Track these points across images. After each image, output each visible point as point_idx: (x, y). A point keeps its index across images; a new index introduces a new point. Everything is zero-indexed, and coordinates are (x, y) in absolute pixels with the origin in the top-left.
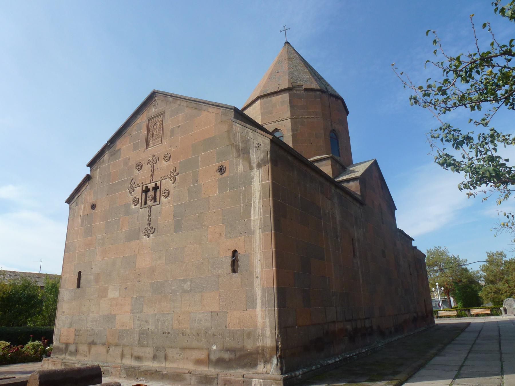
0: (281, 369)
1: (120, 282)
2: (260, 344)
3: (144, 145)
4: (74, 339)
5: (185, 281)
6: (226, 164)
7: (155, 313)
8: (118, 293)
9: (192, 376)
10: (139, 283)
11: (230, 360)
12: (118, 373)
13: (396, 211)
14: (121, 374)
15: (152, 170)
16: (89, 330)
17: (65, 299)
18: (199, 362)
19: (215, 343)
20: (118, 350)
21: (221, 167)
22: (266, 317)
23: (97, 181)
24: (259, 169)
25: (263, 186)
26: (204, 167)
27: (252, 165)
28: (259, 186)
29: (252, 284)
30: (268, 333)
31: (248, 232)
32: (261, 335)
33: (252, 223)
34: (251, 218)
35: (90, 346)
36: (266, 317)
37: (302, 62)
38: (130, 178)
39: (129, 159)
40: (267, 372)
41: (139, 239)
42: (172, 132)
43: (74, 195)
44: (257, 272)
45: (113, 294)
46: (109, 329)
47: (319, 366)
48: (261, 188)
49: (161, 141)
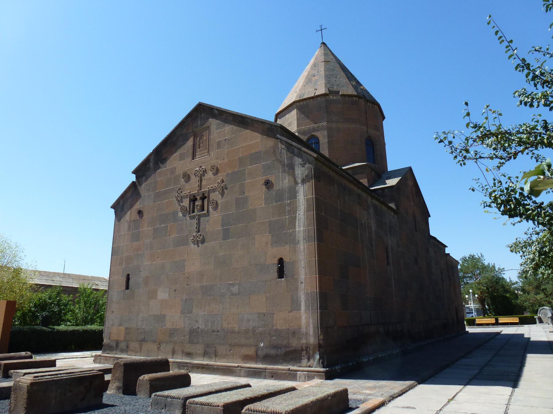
0: (323, 363)
2: (304, 341)
3: (191, 156)
4: (125, 337)
6: (272, 179)
7: (205, 313)
8: (168, 295)
10: (189, 286)
11: (277, 356)
13: (429, 218)
15: (199, 180)
16: (139, 329)
18: (247, 358)
19: (262, 341)
20: (170, 347)
21: (267, 181)
22: (310, 318)
23: (143, 189)
24: (303, 185)
25: (308, 200)
26: (250, 179)
27: (297, 180)
28: (304, 200)
29: (297, 289)
30: (311, 332)
31: (293, 241)
32: (305, 334)
33: (297, 234)
34: (296, 229)
35: (141, 343)
36: (310, 318)
37: (338, 65)
38: (177, 187)
39: (176, 168)
40: (310, 365)
41: (187, 245)
42: (219, 144)
43: (120, 201)
44: (301, 278)
45: (162, 295)
47: (355, 363)
48: (305, 202)
49: (207, 152)
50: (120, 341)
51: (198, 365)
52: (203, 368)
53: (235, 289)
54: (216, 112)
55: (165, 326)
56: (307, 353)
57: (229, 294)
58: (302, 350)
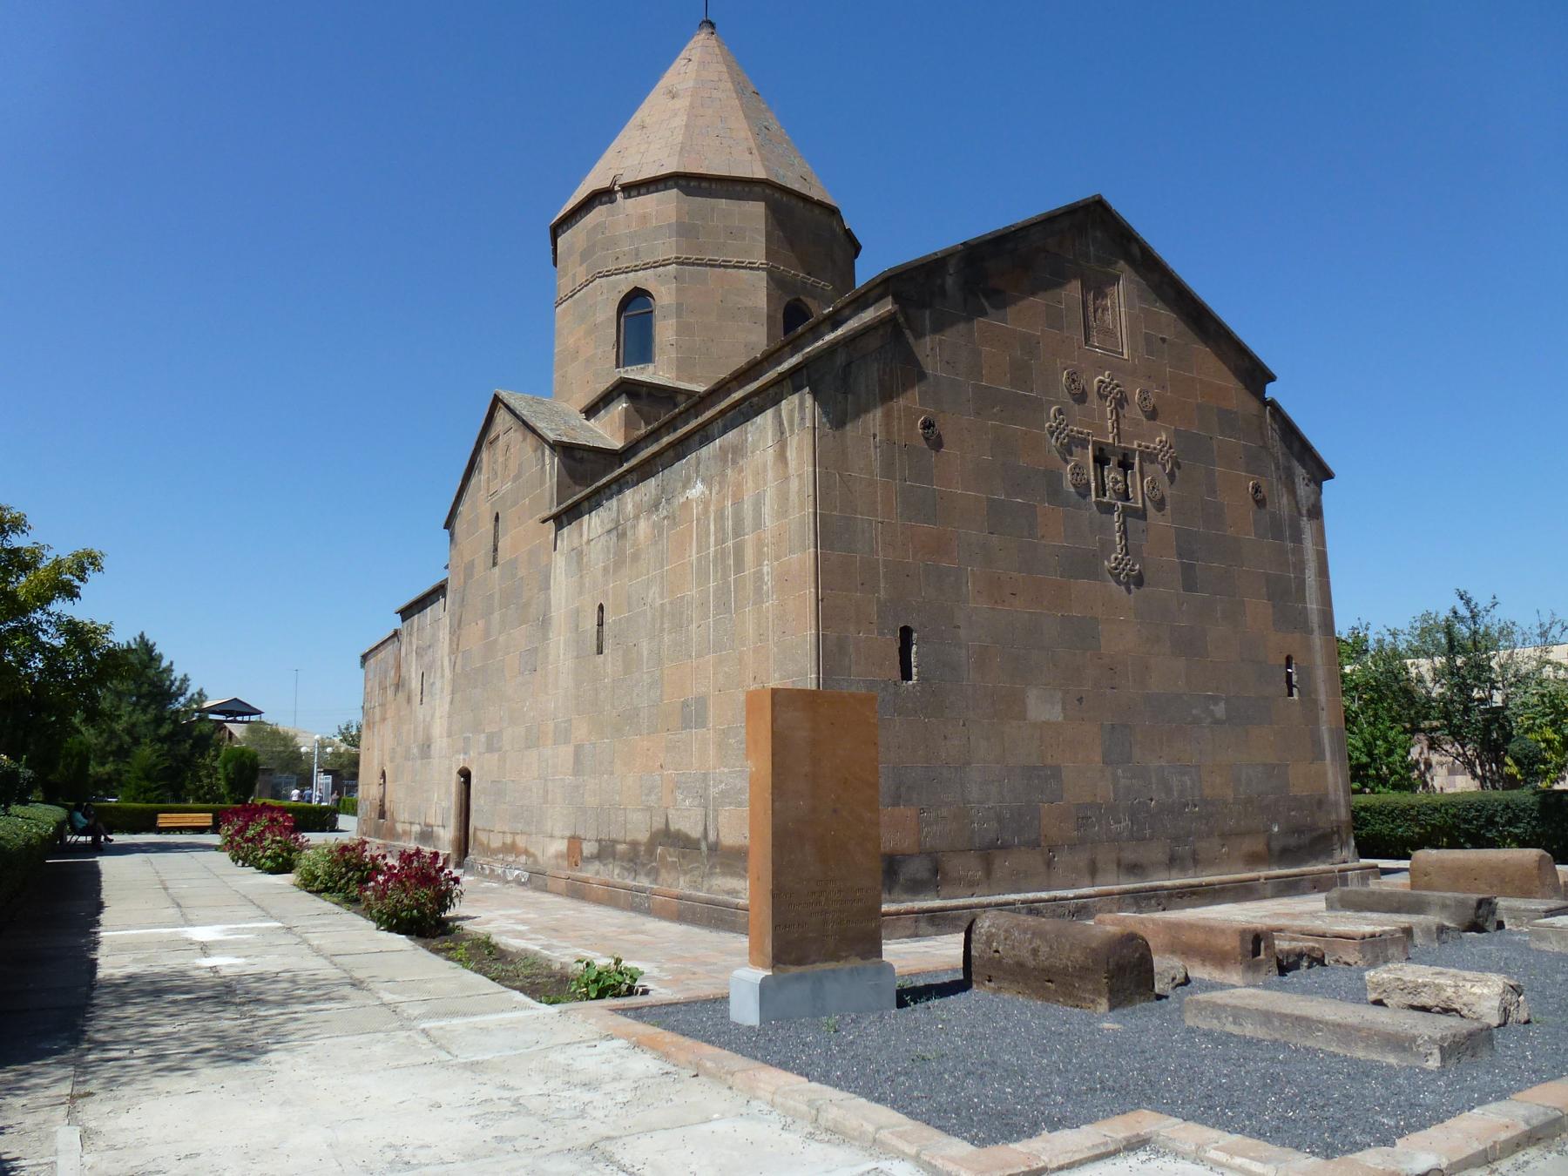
2: (1333, 817)
5: (1215, 700)
10: (1115, 691)
11: (1299, 848)
12: (1115, 908)
19: (1274, 820)
20: (1082, 858)
29: (1316, 720)
45: (1043, 708)
50: (903, 855)
51: (1182, 888)
52: (1193, 893)
54: (1136, 251)
57: (1209, 720)
58: (1333, 833)
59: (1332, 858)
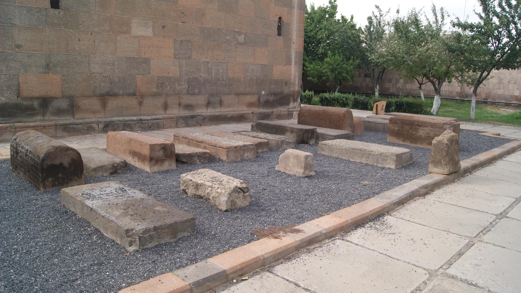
1: (153, 16)
2: (292, 89)
5: (240, 33)
7: (208, 60)
8: (151, 31)
9: (254, 115)
12: (173, 125)
14: (179, 124)
17: (17, 22)
18: (251, 105)
19: (264, 89)
20: (159, 102)
29: (290, 47)
30: (297, 82)
46: (140, 76)
53: (241, 39)
55: (149, 73)
56: (294, 97)
57: (235, 42)
59: (289, 106)
